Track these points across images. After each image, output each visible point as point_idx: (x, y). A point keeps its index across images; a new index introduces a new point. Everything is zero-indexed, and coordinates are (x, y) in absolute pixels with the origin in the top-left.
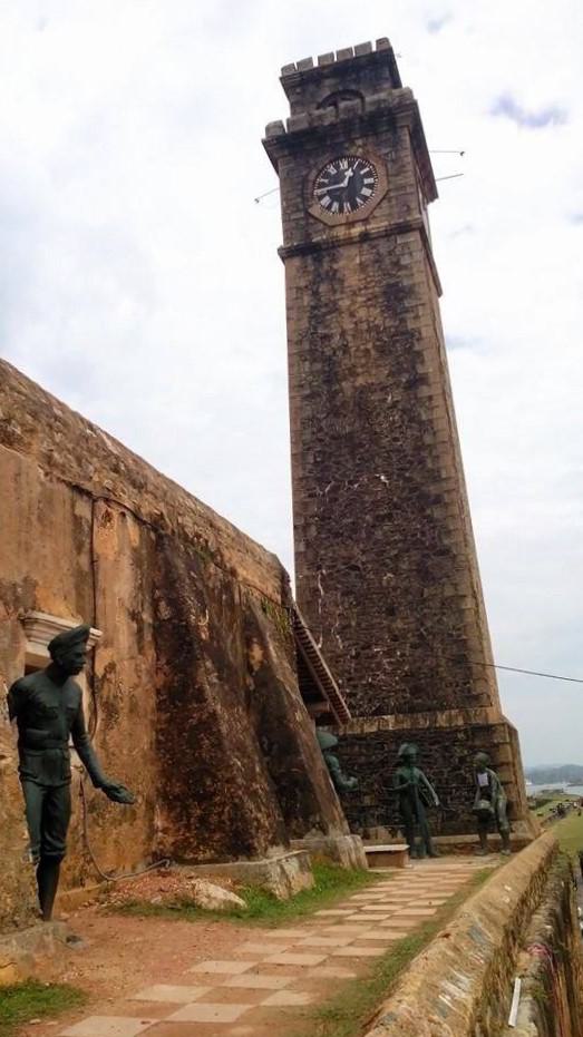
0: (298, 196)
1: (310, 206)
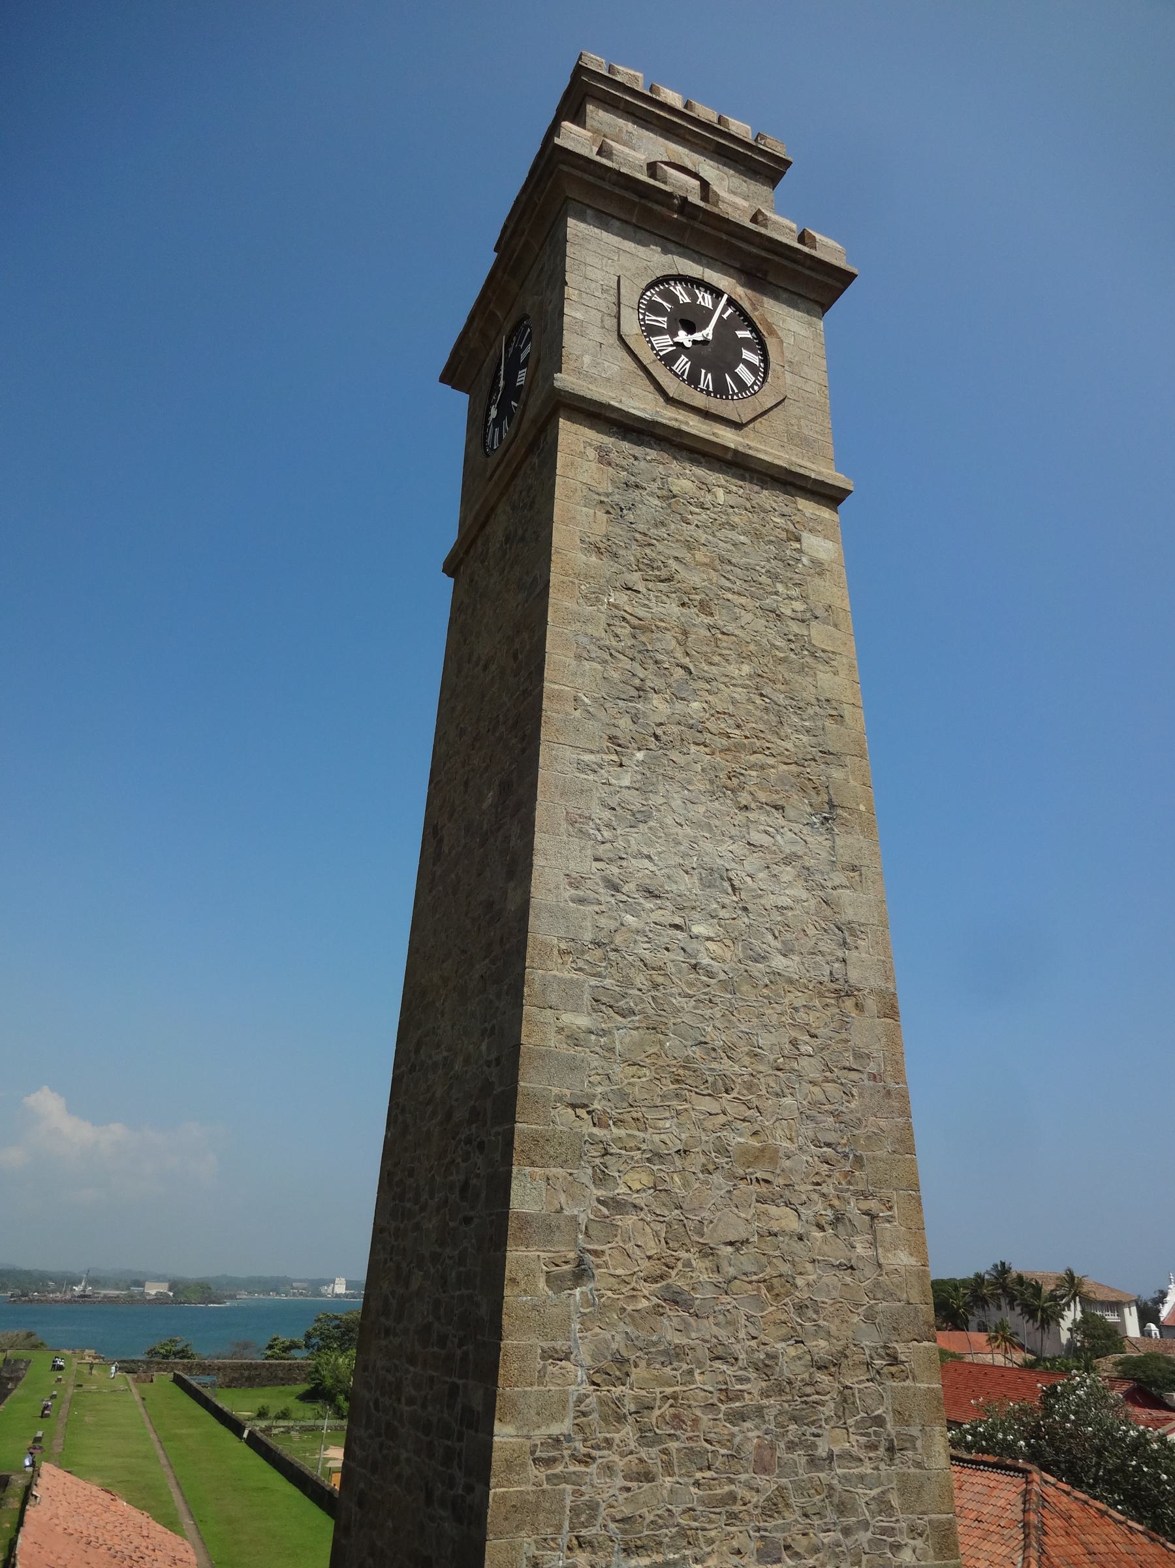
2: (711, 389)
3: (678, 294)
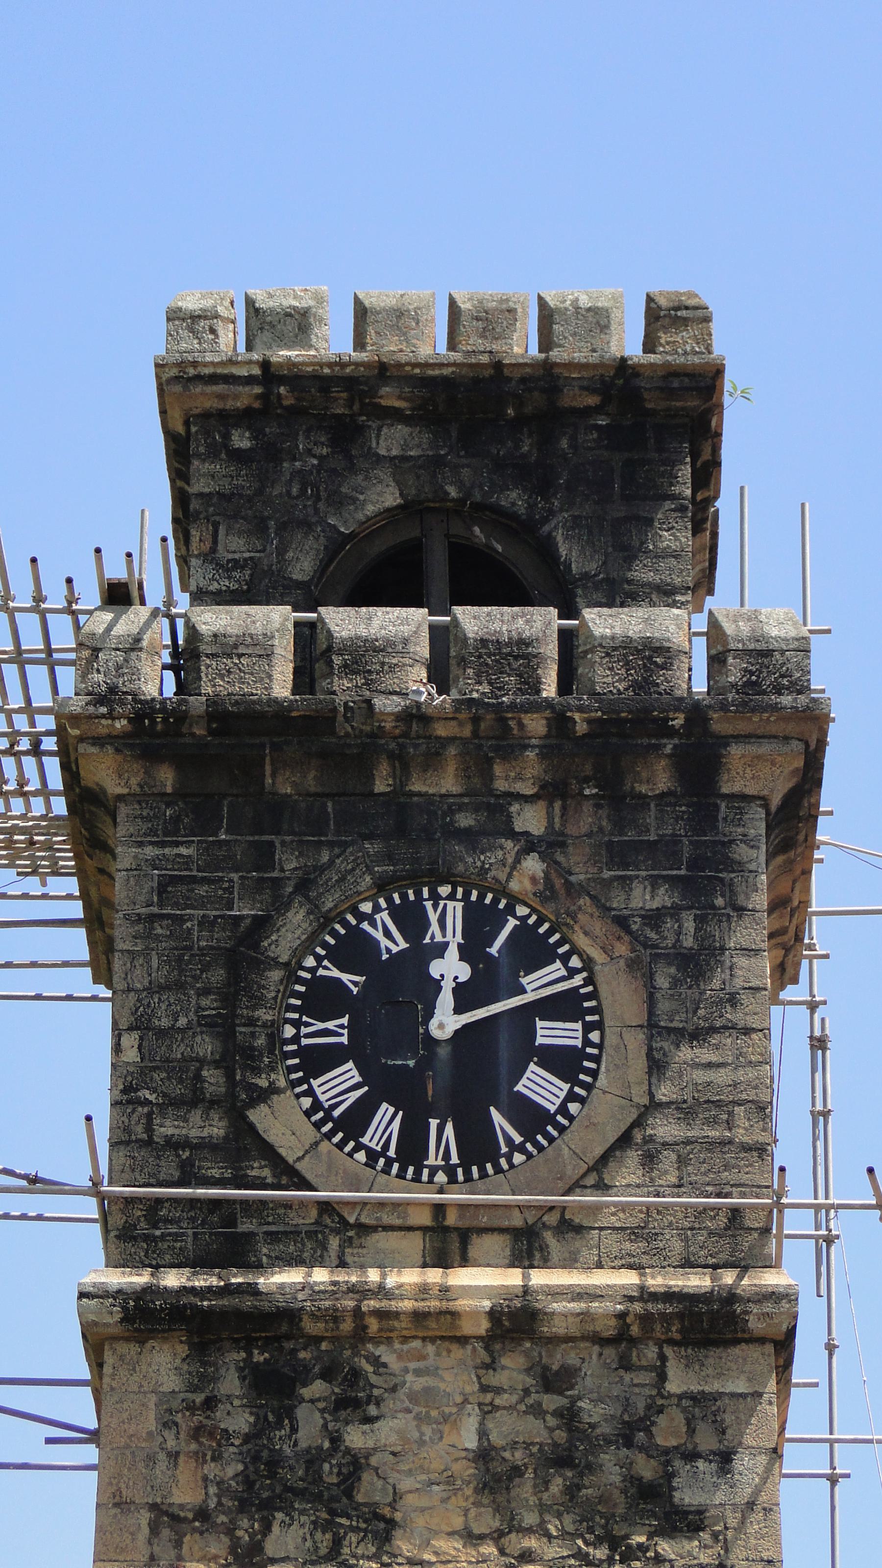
0: (208, 1024)
1: (264, 1095)
2: (455, 1159)
3: (379, 935)
